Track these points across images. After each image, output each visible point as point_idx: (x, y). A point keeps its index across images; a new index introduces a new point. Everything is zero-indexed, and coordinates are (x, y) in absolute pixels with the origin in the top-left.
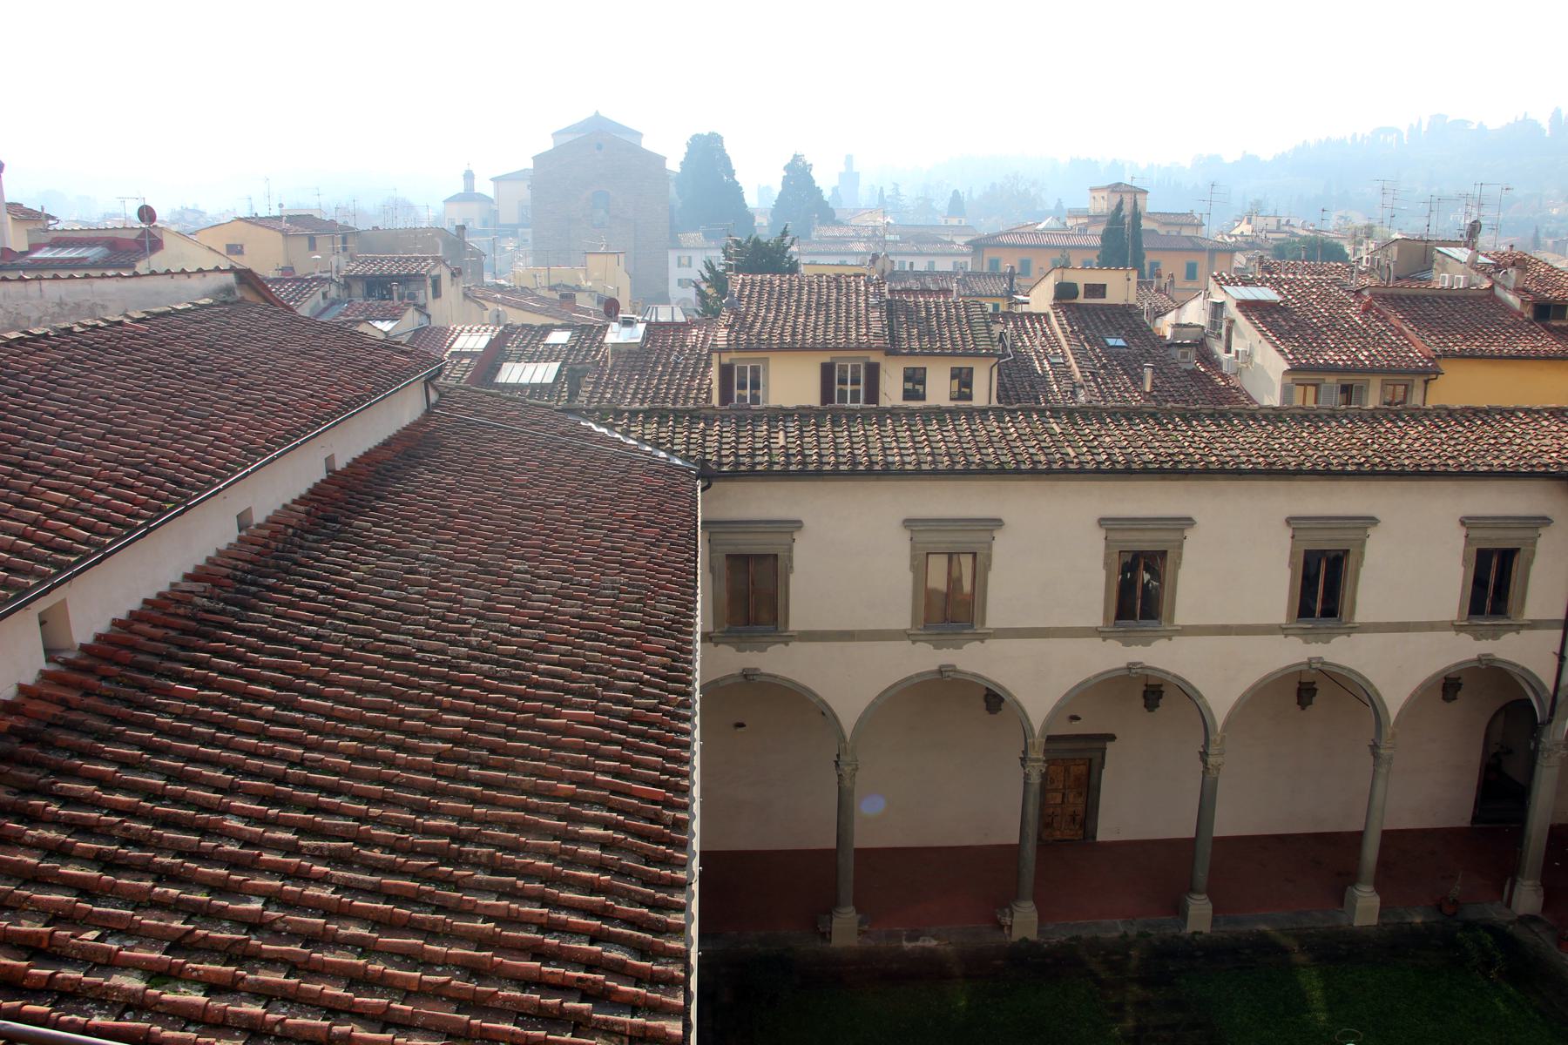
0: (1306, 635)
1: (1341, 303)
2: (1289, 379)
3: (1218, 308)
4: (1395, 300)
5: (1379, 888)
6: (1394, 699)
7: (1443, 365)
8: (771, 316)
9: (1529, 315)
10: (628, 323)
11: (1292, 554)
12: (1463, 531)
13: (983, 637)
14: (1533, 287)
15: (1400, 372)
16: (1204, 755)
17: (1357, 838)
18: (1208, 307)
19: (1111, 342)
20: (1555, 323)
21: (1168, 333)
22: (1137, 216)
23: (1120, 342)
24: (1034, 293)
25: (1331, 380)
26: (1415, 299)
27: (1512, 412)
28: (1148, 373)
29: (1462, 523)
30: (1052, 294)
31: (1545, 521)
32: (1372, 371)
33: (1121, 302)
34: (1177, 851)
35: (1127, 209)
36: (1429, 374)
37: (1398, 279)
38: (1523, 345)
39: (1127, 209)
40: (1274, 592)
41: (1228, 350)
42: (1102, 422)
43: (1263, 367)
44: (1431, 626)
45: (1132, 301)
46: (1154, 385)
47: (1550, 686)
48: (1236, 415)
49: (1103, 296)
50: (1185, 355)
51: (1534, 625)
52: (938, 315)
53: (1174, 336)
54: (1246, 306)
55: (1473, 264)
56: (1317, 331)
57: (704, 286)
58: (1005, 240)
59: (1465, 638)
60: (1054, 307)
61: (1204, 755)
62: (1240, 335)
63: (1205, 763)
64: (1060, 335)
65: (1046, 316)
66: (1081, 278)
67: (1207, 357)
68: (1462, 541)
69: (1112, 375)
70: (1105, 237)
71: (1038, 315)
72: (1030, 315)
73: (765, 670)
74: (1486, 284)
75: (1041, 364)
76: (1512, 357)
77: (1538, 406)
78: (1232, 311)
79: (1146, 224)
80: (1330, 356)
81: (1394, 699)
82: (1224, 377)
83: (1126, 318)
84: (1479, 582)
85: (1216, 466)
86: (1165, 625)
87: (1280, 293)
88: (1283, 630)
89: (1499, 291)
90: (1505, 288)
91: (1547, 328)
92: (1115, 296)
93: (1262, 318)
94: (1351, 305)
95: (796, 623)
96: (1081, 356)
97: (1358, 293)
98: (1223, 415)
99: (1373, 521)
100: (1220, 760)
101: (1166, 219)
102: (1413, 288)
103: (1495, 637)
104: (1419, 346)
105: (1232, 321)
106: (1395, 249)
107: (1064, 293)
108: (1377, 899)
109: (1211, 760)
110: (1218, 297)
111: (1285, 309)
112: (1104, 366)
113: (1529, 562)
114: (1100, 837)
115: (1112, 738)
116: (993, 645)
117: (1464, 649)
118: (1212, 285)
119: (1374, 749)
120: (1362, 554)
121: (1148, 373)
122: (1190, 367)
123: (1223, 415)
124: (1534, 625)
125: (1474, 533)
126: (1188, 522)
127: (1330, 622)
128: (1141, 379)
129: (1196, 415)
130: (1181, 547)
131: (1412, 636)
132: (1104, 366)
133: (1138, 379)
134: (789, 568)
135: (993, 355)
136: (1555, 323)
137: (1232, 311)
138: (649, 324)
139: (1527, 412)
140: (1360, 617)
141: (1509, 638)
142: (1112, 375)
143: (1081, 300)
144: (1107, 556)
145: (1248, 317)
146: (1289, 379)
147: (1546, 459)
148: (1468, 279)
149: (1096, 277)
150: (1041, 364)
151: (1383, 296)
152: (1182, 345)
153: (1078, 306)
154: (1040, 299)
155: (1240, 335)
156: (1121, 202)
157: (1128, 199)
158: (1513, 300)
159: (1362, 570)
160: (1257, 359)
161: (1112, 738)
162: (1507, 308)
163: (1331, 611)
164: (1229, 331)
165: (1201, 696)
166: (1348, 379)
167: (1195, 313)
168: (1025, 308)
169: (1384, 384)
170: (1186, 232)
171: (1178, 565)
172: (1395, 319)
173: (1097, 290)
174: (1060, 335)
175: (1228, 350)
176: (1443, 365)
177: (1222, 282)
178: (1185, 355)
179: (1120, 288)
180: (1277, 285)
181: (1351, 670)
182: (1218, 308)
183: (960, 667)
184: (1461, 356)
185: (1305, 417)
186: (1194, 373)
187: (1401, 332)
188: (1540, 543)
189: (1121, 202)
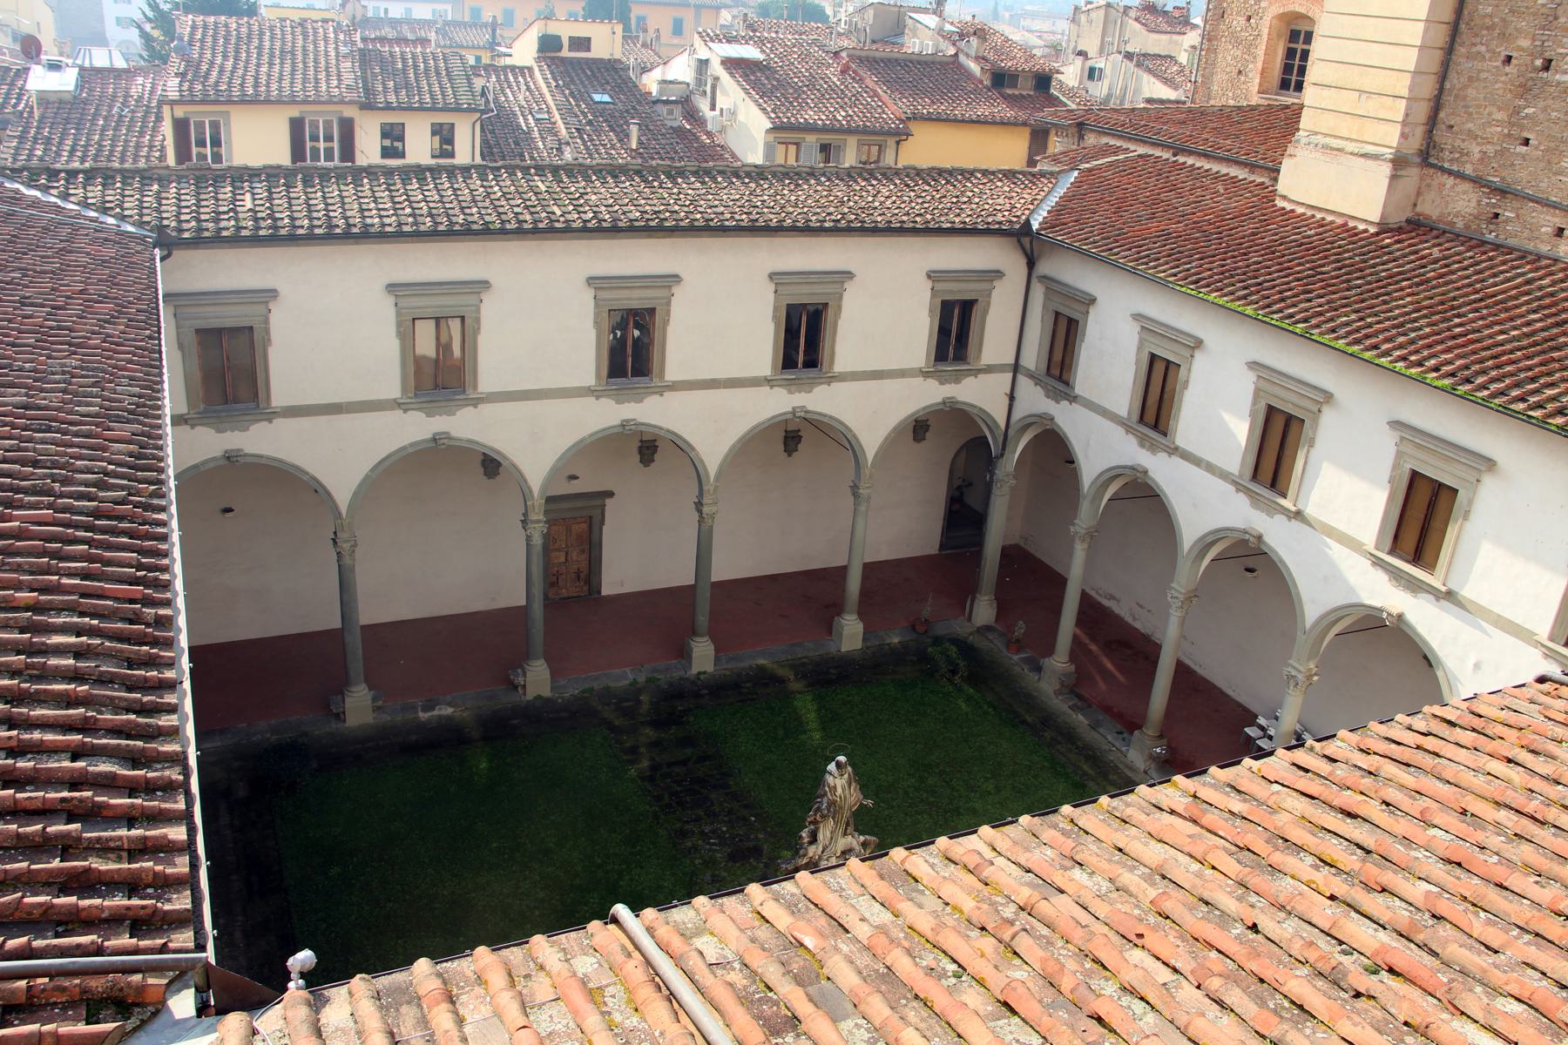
0: (790, 385)
1: (820, 64)
2: (771, 137)
3: (703, 64)
4: (870, 63)
5: (862, 615)
6: (871, 441)
7: (914, 127)
8: (229, 64)
9: (987, 82)
11: (776, 309)
12: (929, 284)
13: (476, 402)
14: (991, 56)
15: (874, 133)
16: (699, 505)
17: (842, 572)
18: (693, 64)
19: (597, 97)
20: (1009, 91)
21: (654, 89)
23: (606, 98)
24: (517, 45)
25: (811, 139)
26: (890, 63)
27: (972, 173)
28: (634, 130)
29: (929, 277)
30: (535, 46)
31: (998, 274)
32: (850, 131)
33: (606, 56)
34: (679, 597)
36: (901, 135)
37: (874, 42)
38: (982, 110)
40: (759, 346)
41: (713, 108)
42: (588, 180)
43: (746, 127)
44: (902, 373)
45: (618, 56)
46: (640, 143)
47: (1003, 425)
48: (720, 172)
49: (589, 50)
50: (670, 112)
51: (989, 369)
52: (416, 67)
53: (661, 92)
54: (731, 64)
55: (940, 32)
56: (798, 90)
57: (148, 27)
59: (932, 383)
60: (538, 60)
61: (699, 505)
62: (726, 93)
63: (700, 512)
64: (545, 90)
65: (530, 69)
67: (692, 115)
68: (929, 293)
69: (598, 132)
71: (522, 69)
72: (513, 68)
73: (249, 449)
74: (952, 51)
75: (526, 120)
76: (972, 122)
77: (993, 168)
78: (717, 68)
80: (810, 116)
81: (871, 441)
82: (709, 134)
83: (611, 73)
84: (943, 331)
85: (701, 223)
86: (656, 382)
87: (763, 51)
88: (768, 382)
89: (962, 58)
90: (967, 55)
91: (1005, 97)
92: (599, 51)
93: (745, 76)
94: (830, 65)
95: (280, 396)
96: (566, 112)
97: (836, 54)
98: (707, 172)
99: (849, 275)
100: (714, 509)
102: (886, 51)
103: (957, 381)
104: (893, 108)
105: (717, 79)
106: (871, 12)
107: (548, 45)
108: (861, 626)
109: (706, 510)
110: (703, 53)
111: (767, 67)
112: (590, 123)
113: (986, 312)
114: (604, 592)
115: (610, 494)
116: (485, 408)
117: (929, 394)
119: (855, 489)
120: (840, 307)
121: (634, 130)
122: (675, 124)
123: (707, 172)
124: (989, 369)
125: (939, 286)
126: (676, 278)
127: (812, 372)
128: (627, 136)
129: (681, 173)
130: (669, 304)
131: (887, 384)
132: (590, 123)
133: (624, 136)
134: (267, 341)
135: (475, 110)
136: (1009, 91)
137: (717, 68)
139: (985, 173)
140: (839, 367)
141: (969, 381)
142: (598, 132)
143: (565, 53)
144: (597, 315)
146: (771, 137)
147: (999, 217)
148: (936, 46)
149: (581, 30)
150: (526, 120)
151: (860, 58)
152: (667, 102)
153: (563, 60)
154: (524, 52)
155: (726, 93)
158: (974, 67)
159: (840, 323)
160: (741, 117)
161: (610, 494)
162: (969, 75)
163: (812, 362)
164: (714, 88)
165: (693, 449)
166: (827, 138)
167: (680, 70)
168: (508, 61)
169: (860, 144)
171: (666, 322)
172: (871, 80)
173: (582, 43)
174: (545, 90)
175: (713, 108)
176: (914, 127)
177: (708, 38)
178: (670, 112)
180: (760, 43)
181: (831, 417)
182: (703, 64)
183: (454, 434)
184: (929, 119)
185: (786, 175)
186: (679, 131)
187: (876, 94)
188: (995, 294)
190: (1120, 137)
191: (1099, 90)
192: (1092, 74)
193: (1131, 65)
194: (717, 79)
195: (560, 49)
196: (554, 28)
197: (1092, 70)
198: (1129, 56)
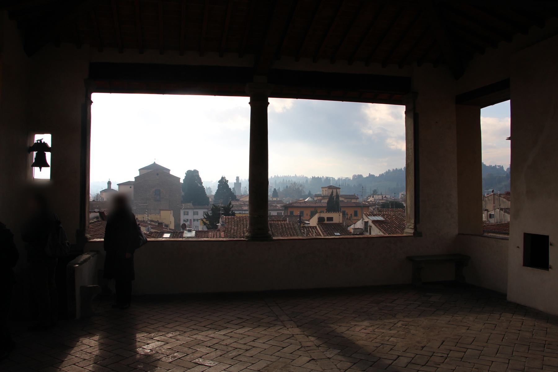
3: (366, 223)
8: (236, 228)
10: (190, 231)
21: (352, 231)
22: (338, 196)
24: (311, 220)
30: (317, 220)
35: (334, 194)
39: (334, 194)
52: (285, 227)
53: (354, 232)
54: (374, 222)
57: (205, 220)
58: (295, 205)
60: (318, 224)
64: (321, 233)
65: (316, 227)
66: (326, 215)
70: (328, 203)
71: (313, 227)
72: (311, 227)
79: (341, 199)
101: (346, 197)
105: (371, 227)
107: (321, 220)
110: (366, 220)
118: (364, 216)
137: (370, 223)
138: (196, 232)
143: (326, 222)
145: (375, 225)
154: (313, 222)
156: (332, 192)
157: (335, 191)
164: (370, 229)
167: (359, 225)
168: (308, 225)
170: (353, 201)
173: (330, 219)
174: (321, 233)
177: (367, 215)
179: (337, 218)
182: (366, 223)
189: (332, 192)
190: (494, 233)
191: (492, 221)
192: (491, 216)
193: (502, 212)
194: (371, 227)
195: (324, 221)
196: (323, 215)
197: (490, 215)
198: (501, 209)
